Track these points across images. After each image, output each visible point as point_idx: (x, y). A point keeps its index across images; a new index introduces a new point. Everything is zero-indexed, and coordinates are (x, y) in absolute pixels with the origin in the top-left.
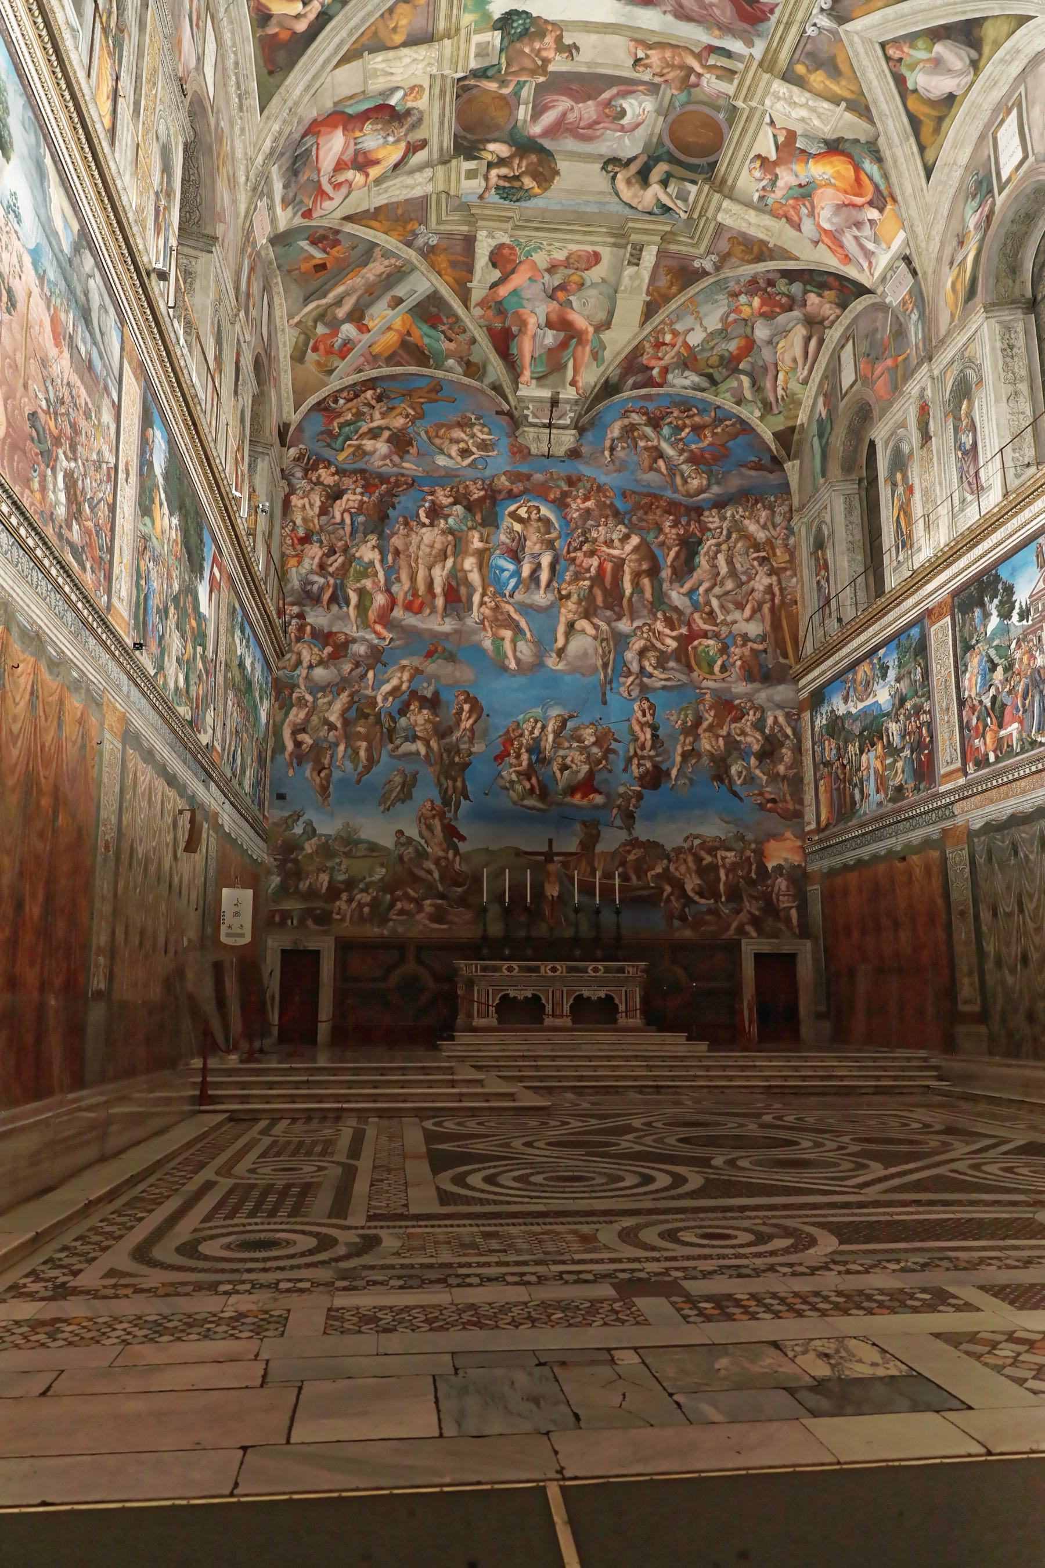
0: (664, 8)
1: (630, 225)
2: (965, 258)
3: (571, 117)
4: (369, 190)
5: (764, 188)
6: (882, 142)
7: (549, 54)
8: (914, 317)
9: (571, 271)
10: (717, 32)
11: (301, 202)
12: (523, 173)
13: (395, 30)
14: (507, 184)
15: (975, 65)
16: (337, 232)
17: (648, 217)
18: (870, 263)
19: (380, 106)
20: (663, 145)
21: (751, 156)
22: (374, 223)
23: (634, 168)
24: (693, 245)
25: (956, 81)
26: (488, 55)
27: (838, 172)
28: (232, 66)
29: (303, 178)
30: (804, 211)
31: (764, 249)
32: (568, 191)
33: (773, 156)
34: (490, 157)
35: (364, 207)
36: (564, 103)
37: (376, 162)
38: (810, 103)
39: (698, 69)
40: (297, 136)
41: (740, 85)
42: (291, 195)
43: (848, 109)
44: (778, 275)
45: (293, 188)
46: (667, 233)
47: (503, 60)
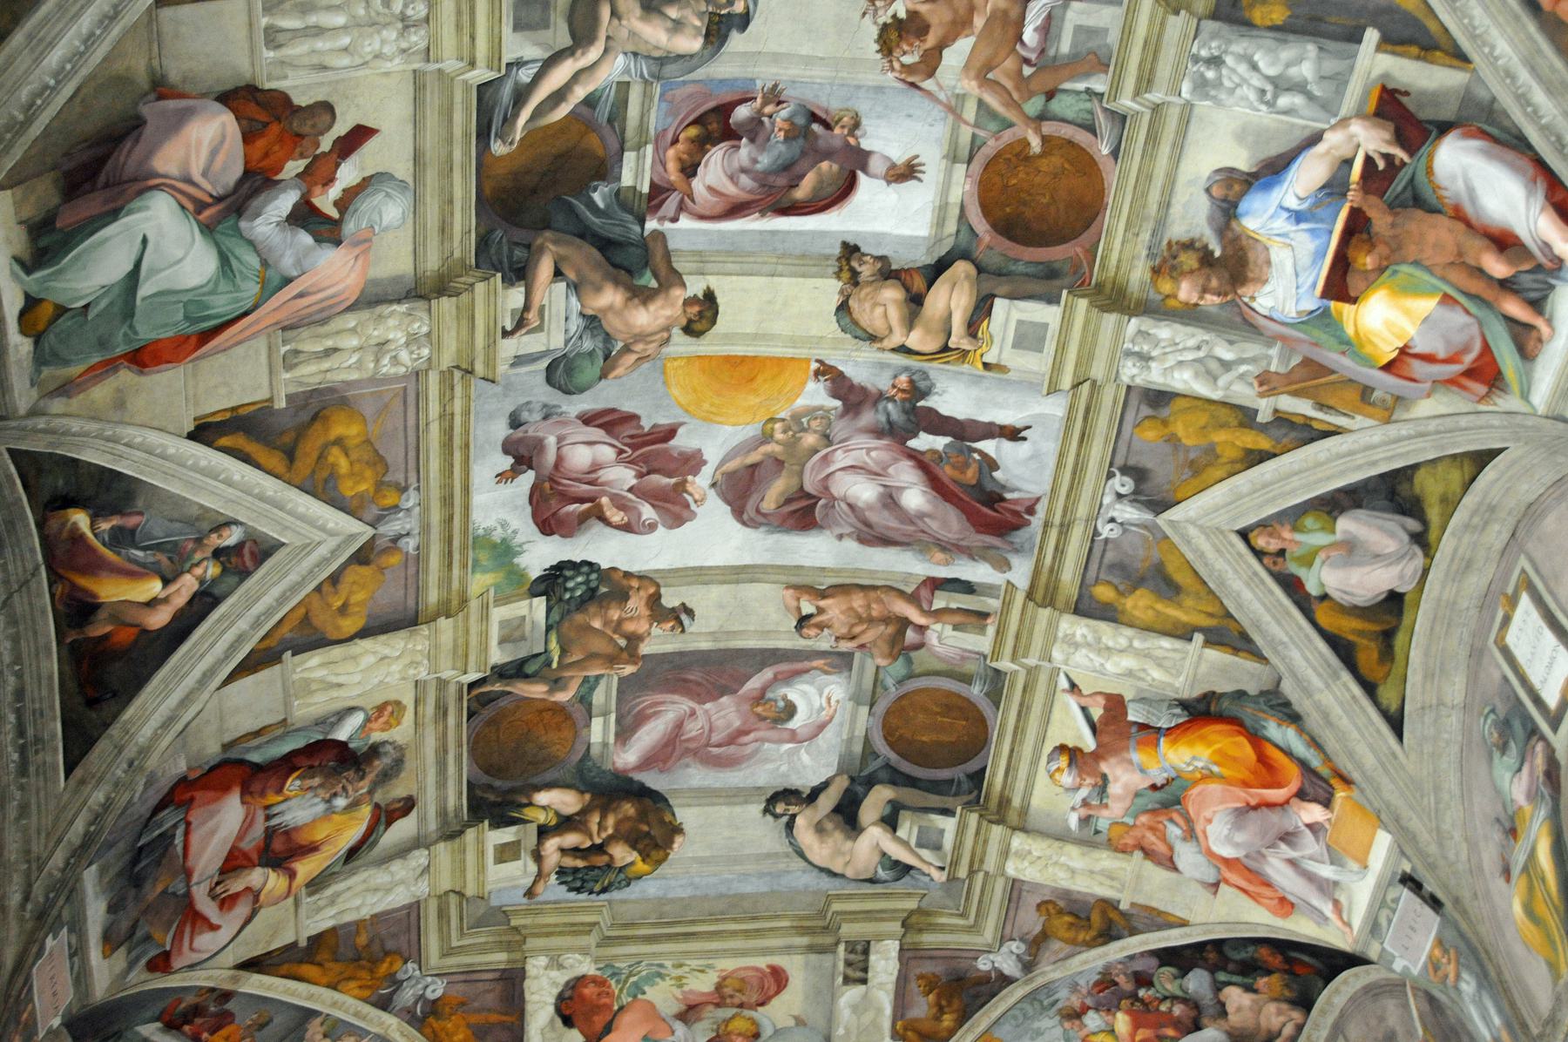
0: (838, 531)
2: (1532, 855)
3: (693, 729)
4: (297, 904)
5: (1085, 803)
6: (1288, 688)
7: (641, 627)
8: (1468, 986)
9: (728, 1013)
10: (940, 556)
11: (148, 938)
12: (611, 838)
13: (343, 610)
14: (580, 863)
15: (1422, 541)
16: (226, 996)
17: (868, 889)
18: (1336, 903)
19: (318, 742)
21: (1048, 748)
22: (308, 970)
23: (827, 802)
24: (969, 930)
25: (1395, 570)
26: (523, 638)
27: (1219, 752)
28: (9, 698)
29: (152, 891)
30: (1174, 832)
31: (1113, 915)
32: (701, 861)
33: (1089, 743)
34: (542, 817)
37: (312, 848)
38: (1136, 644)
39: (921, 620)
40: (144, 810)
41: (1000, 633)
42: (125, 925)
43: (1208, 643)
44: (1154, 962)
45: (132, 910)
46: (912, 913)
47: (554, 645)
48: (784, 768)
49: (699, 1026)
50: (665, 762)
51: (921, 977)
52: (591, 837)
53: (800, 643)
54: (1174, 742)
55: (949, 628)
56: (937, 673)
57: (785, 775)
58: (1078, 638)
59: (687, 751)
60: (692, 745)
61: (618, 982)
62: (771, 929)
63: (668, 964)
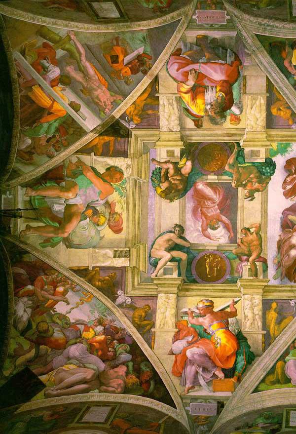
1: (142, 247)
3: (209, 203)
4: (173, 94)
5: (193, 312)
10: (276, 262)
12: (171, 182)
14: (162, 174)
17: (147, 255)
20: (198, 253)
21: (210, 299)
23: (179, 241)
24: (133, 286)
27: (225, 346)
30: (190, 339)
31: (148, 327)
32: (160, 209)
33: (216, 310)
34: (182, 163)
35: (161, 89)
36: (217, 198)
38: (257, 317)
39: (251, 259)
43: (264, 336)
44: (130, 343)
46: (138, 269)
48: (192, 229)
49: (103, 208)
50: (196, 196)
51: (115, 274)
52: (171, 177)
53: (239, 230)
54: (225, 332)
55: (250, 267)
56: (232, 266)
57: (189, 229)
58: (254, 301)
59: (200, 202)
60: (202, 203)
61: (120, 184)
62: (135, 228)
63: (125, 198)
